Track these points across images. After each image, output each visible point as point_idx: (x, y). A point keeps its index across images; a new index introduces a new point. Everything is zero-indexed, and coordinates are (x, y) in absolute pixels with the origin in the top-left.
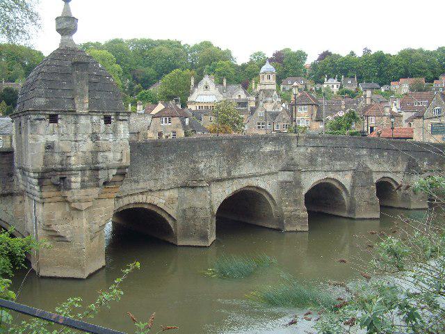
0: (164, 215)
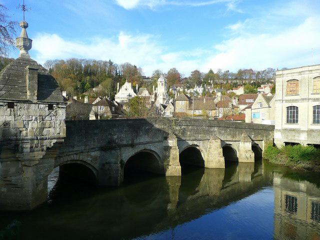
0: (90, 167)
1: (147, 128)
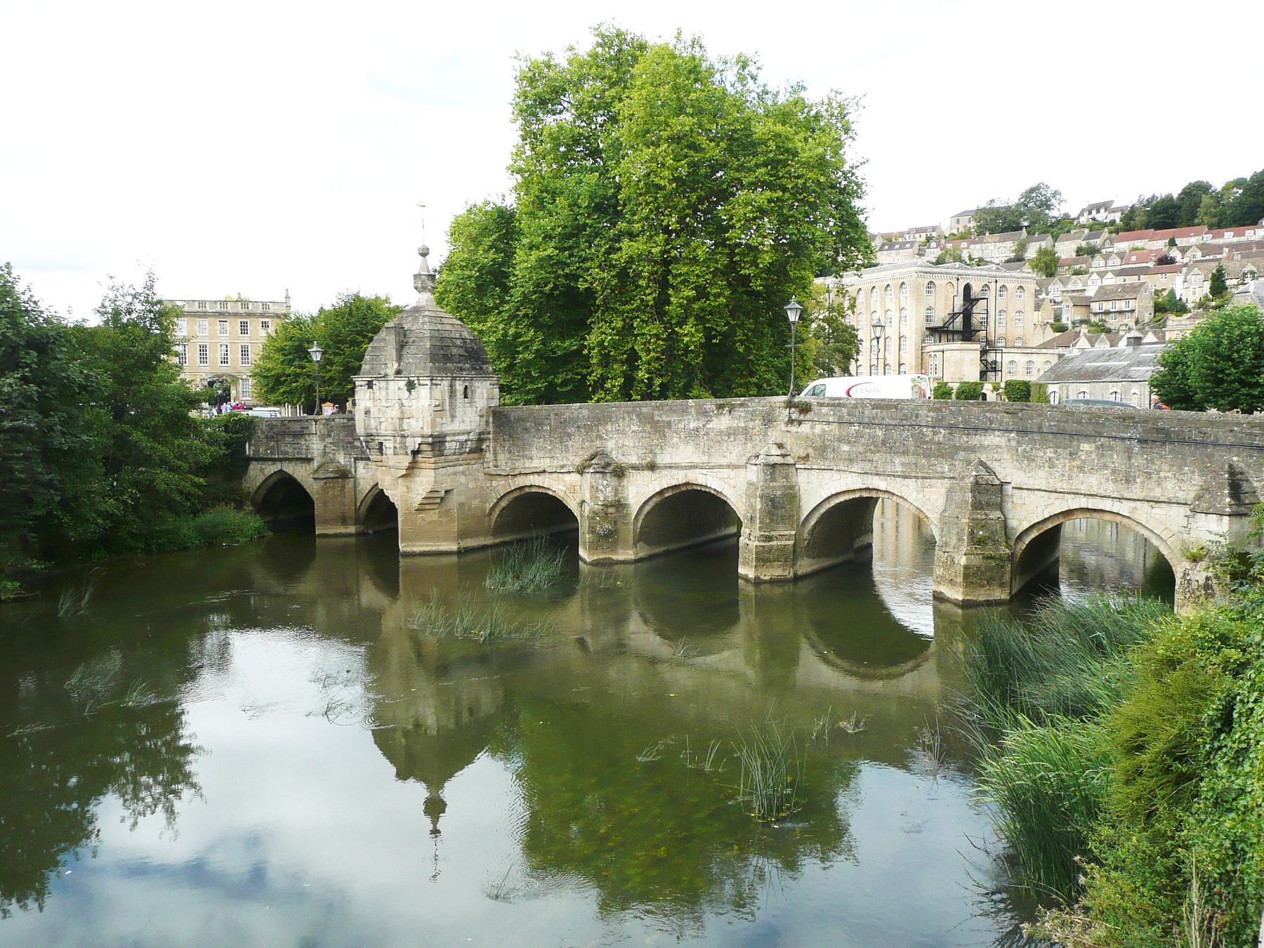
1: (692, 425)
